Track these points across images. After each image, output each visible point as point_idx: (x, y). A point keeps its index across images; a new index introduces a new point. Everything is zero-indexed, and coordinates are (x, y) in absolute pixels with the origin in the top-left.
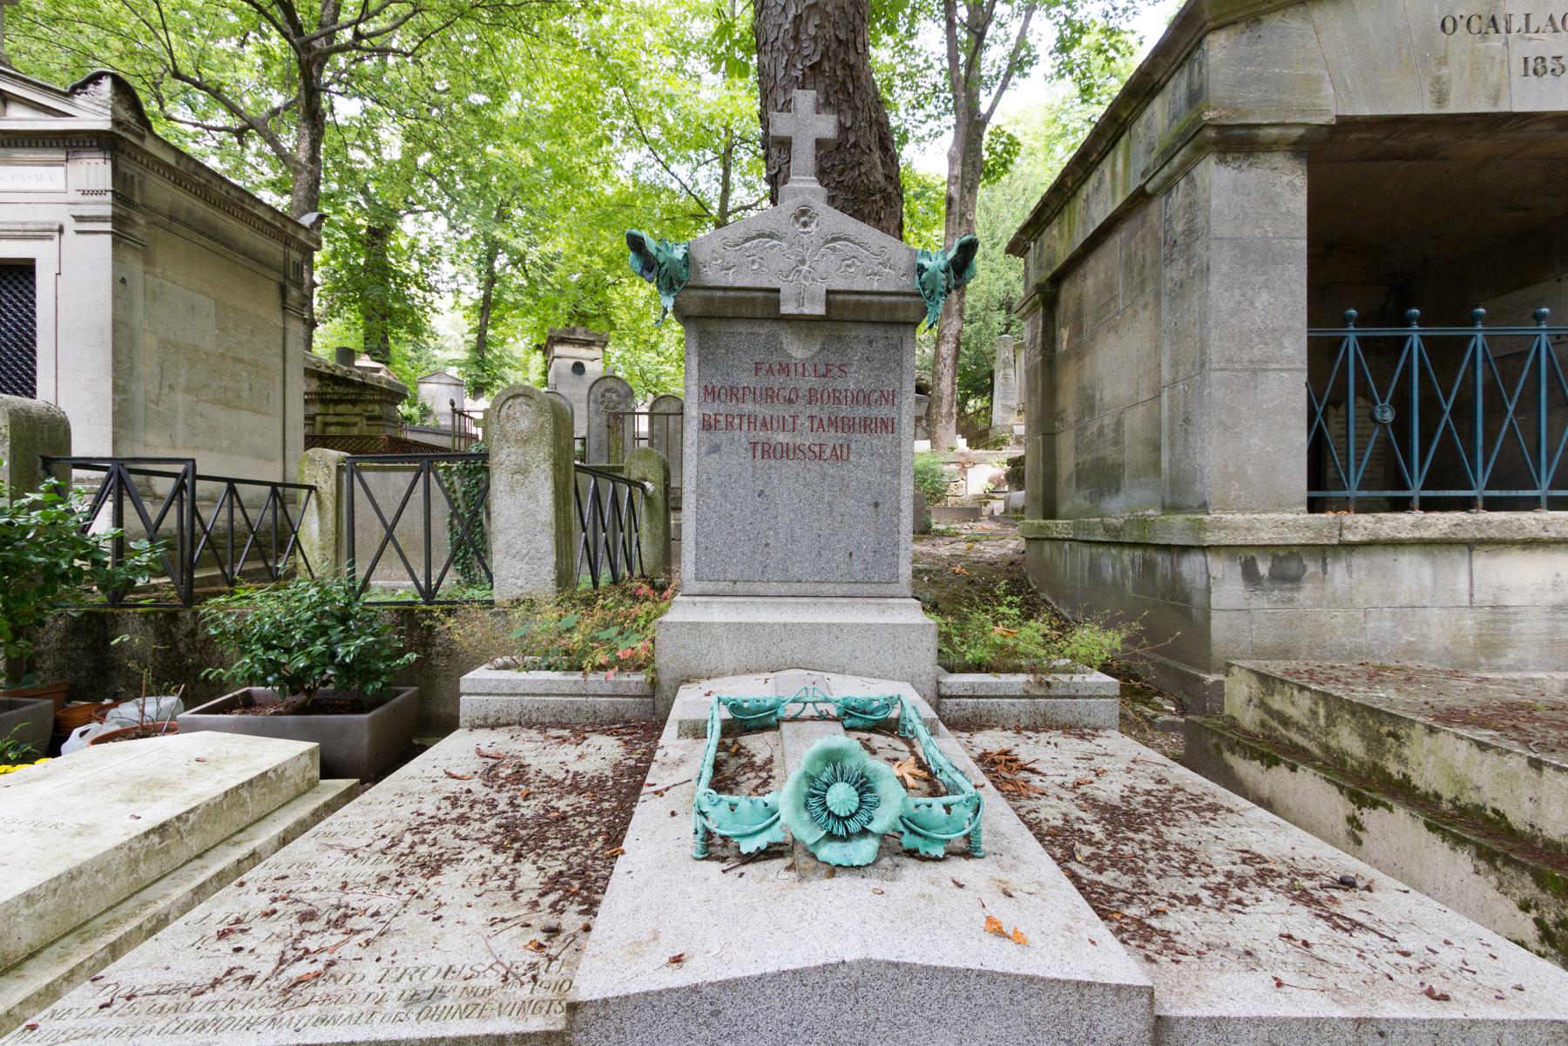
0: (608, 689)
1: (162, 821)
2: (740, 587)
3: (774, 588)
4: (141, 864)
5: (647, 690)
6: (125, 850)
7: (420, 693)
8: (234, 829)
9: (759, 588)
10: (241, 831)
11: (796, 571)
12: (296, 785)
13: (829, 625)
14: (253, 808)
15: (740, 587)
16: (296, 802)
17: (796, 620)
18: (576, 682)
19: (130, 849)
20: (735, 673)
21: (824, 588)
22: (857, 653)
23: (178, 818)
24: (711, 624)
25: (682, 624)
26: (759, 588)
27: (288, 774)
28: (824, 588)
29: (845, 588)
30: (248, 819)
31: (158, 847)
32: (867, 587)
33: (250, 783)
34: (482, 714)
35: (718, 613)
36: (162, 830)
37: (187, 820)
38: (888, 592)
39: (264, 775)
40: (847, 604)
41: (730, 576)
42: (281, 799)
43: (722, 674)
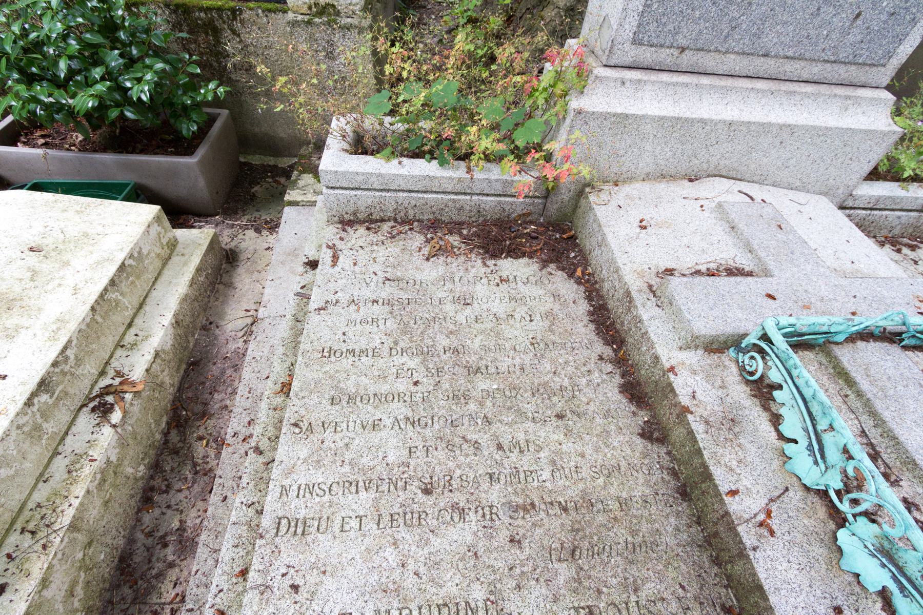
0: (498, 188)
1: (37, 379)
2: (687, 59)
3: (732, 63)
4: (45, 425)
6: (14, 433)
7: (231, 113)
8: (122, 329)
9: (709, 61)
10: (130, 325)
11: (770, 40)
12: (158, 255)
13: (782, 127)
14: (129, 301)
15: (687, 59)
16: (167, 273)
17: (746, 117)
19: (18, 427)
20: (647, 178)
21: (791, 68)
22: (792, 162)
23: (55, 364)
25: (606, 116)
26: (709, 61)
27: (145, 251)
28: (791, 68)
29: (816, 70)
30: (129, 313)
31: (50, 401)
32: (842, 69)
33: (112, 283)
34: (351, 209)
35: (652, 100)
36: (44, 385)
37: (67, 358)
38: (863, 79)
39: (122, 267)
40: (816, 96)
41: (681, 41)
42: (151, 276)
43: (631, 179)
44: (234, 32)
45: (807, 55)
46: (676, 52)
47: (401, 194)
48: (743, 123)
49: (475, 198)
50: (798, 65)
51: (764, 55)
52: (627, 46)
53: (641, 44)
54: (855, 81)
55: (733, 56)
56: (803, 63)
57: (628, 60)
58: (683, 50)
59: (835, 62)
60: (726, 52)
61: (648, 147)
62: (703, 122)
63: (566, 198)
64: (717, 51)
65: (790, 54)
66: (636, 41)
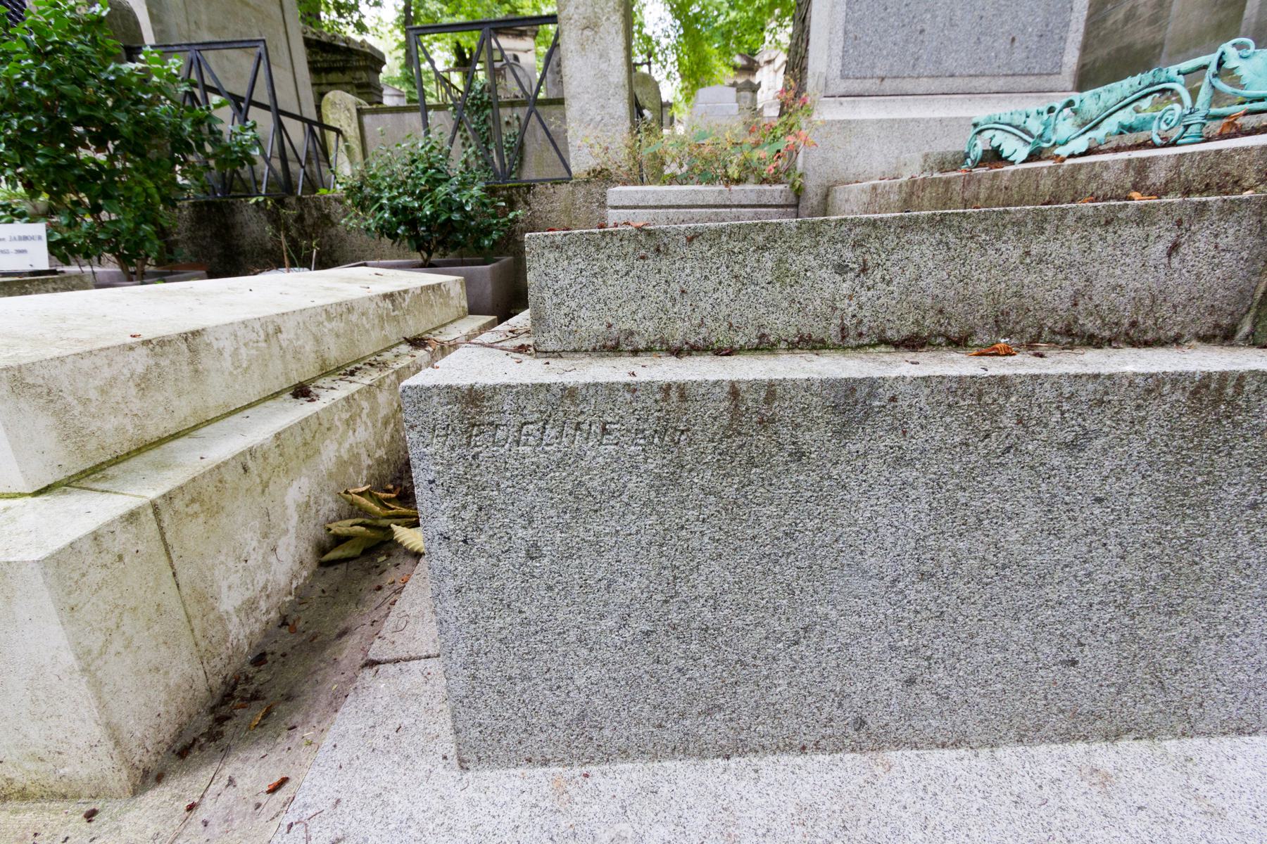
2: (889, 85)
3: (925, 84)
5: (792, 199)
9: (908, 85)
11: (949, 64)
15: (889, 85)
17: (953, 114)
18: (720, 192)
24: (863, 121)
25: (832, 123)
26: (908, 85)
29: (1000, 83)
32: (1025, 80)
38: (1047, 86)
41: (878, 72)
44: (527, 203)
45: (987, 72)
46: (878, 81)
47: (671, 210)
48: (951, 119)
49: (734, 210)
50: (983, 80)
51: (952, 76)
52: (838, 80)
53: (848, 78)
54: (1041, 88)
55: (925, 79)
56: (988, 79)
57: (842, 90)
58: (883, 79)
59: (1013, 75)
60: (918, 77)
61: (876, 147)
62: (913, 120)
63: (815, 203)
64: (910, 77)
65: (972, 72)
66: (844, 77)
